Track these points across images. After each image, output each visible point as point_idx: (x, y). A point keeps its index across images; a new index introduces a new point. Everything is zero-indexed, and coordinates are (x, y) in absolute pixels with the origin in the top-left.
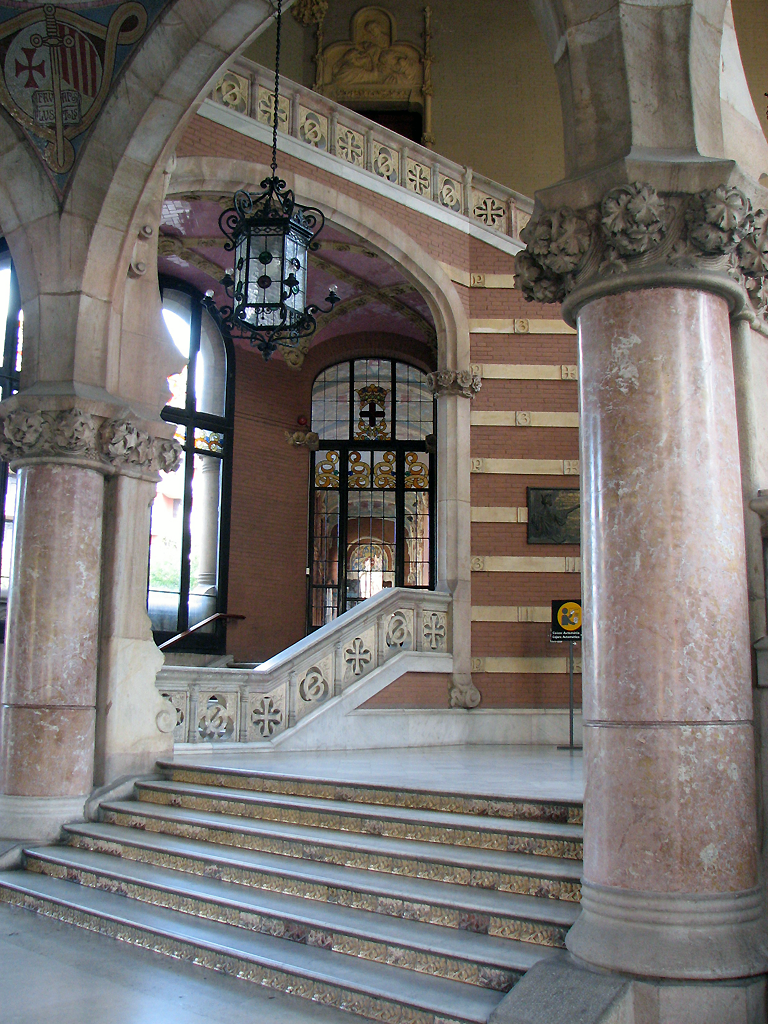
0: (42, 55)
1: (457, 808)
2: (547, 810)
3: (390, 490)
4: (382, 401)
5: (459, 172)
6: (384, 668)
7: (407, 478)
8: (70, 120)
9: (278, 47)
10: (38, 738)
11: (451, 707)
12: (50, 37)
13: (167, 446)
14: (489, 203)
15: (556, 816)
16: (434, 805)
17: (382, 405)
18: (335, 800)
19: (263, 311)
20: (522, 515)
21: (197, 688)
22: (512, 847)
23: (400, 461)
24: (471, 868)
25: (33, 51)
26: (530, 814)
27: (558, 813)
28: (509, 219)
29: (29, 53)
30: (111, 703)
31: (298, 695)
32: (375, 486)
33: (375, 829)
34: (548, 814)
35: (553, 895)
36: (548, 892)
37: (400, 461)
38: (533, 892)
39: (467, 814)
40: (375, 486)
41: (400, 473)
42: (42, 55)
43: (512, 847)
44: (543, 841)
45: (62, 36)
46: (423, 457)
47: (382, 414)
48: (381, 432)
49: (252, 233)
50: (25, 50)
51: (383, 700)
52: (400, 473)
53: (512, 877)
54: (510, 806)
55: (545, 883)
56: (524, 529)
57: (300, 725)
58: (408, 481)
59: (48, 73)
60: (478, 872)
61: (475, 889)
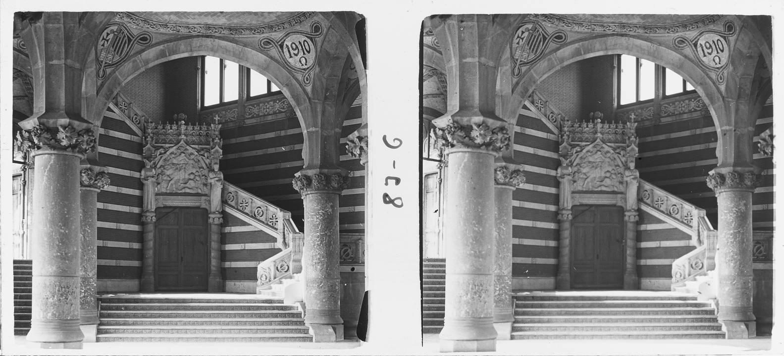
0: (526, 34)
8: (523, 60)
12: (531, 30)
25: (524, 32)
29: (523, 33)
42: (526, 34)
45: (535, 31)
50: (522, 31)
59: (524, 41)
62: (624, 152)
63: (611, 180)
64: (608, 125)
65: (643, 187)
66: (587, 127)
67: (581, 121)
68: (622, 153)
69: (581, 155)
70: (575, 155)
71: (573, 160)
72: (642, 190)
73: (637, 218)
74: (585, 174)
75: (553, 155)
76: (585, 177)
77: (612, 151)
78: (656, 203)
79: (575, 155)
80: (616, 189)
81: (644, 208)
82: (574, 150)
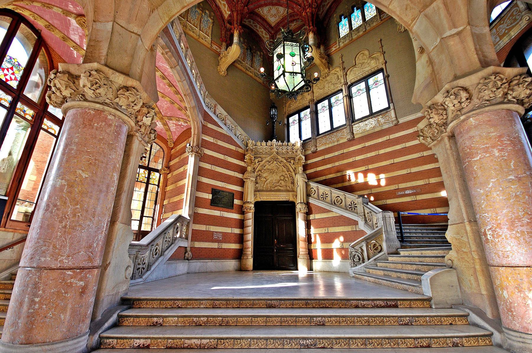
1: (342, 305)
2: (389, 303)
3: (144, 183)
4: (146, 153)
5: (205, 91)
6: (175, 244)
7: (150, 180)
9: (122, 26)
10: (66, 293)
11: (185, 259)
13: (152, 131)
14: (210, 103)
15: (393, 305)
16: (329, 305)
17: (146, 155)
18: (267, 308)
19: (293, 75)
20: (210, 196)
21: (140, 253)
22: (401, 323)
23: (149, 174)
24: (415, 338)
26: (380, 305)
27: (394, 304)
28: (215, 110)
30: (110, 263)
31: (151, 255)
32: (138, 180)
33: (320, 322)
34: (389, 304)
35: (461, 345)
36: (458, 343)
37: (149, 174)
38: (451, 345)
39: (348, 308)
40: (138, 180)
41: (148, 178)
43: (401, 323)
44: (417, 318)
46: (157, 174)
47: (145, 157)
48: (144, 163)
49: (285, 44)
51: (173, 258)
52: (148, 178)
53: (422, 339)
54: (370, 302)
55: (455, 340)
56: (210, 201)
57: (152, 269)
58: (151, 181)
60: (420, 340)
61: (420, 349)
62: (294, 162)
63: (285, 182)
64: (281, 143)
65: (310, 185)
66: (266, 145)
67: (261, 141)
68: (292, 162)
69: (262, 163)
70: (257, 164)
71: (256, 168)
72: (309, 188)
73: (306, 210)
74: (265, 178)
75: (242, 164)
76: (264, 180)
77: (285, 161)
78: (321, 197)
79: (257, 164)
80: (288, 188)
81: (311, 201)
82: (257, 161)
